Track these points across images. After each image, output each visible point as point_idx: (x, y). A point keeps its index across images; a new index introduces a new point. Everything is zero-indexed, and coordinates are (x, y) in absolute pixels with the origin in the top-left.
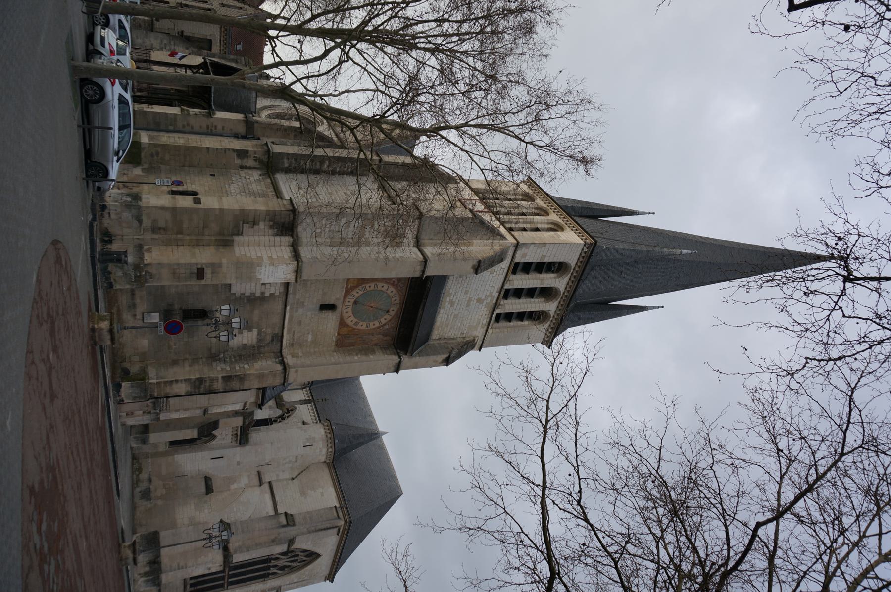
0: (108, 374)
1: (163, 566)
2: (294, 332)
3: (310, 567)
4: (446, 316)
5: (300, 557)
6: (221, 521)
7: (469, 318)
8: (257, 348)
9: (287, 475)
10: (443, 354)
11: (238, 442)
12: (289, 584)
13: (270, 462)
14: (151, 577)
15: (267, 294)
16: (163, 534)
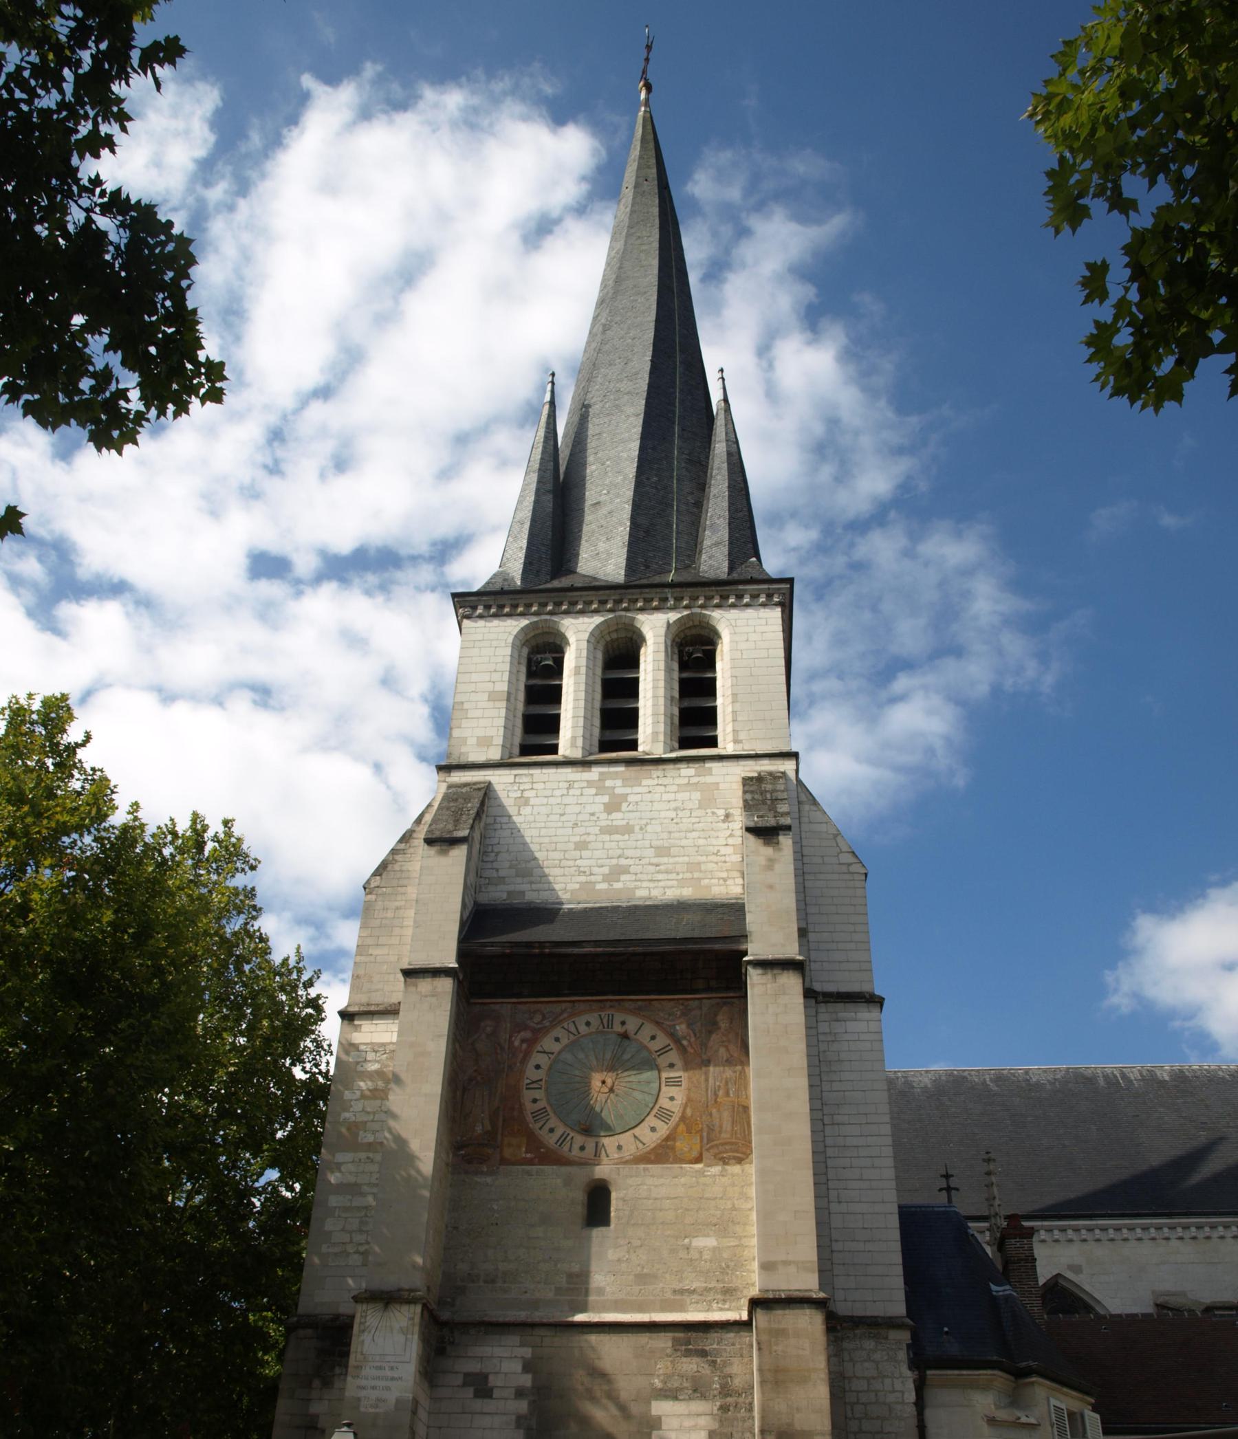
2: (682, 1292)
4: (660, 877)
7: (673, 814)
8: (729, 1399)
15: (527, 1380)
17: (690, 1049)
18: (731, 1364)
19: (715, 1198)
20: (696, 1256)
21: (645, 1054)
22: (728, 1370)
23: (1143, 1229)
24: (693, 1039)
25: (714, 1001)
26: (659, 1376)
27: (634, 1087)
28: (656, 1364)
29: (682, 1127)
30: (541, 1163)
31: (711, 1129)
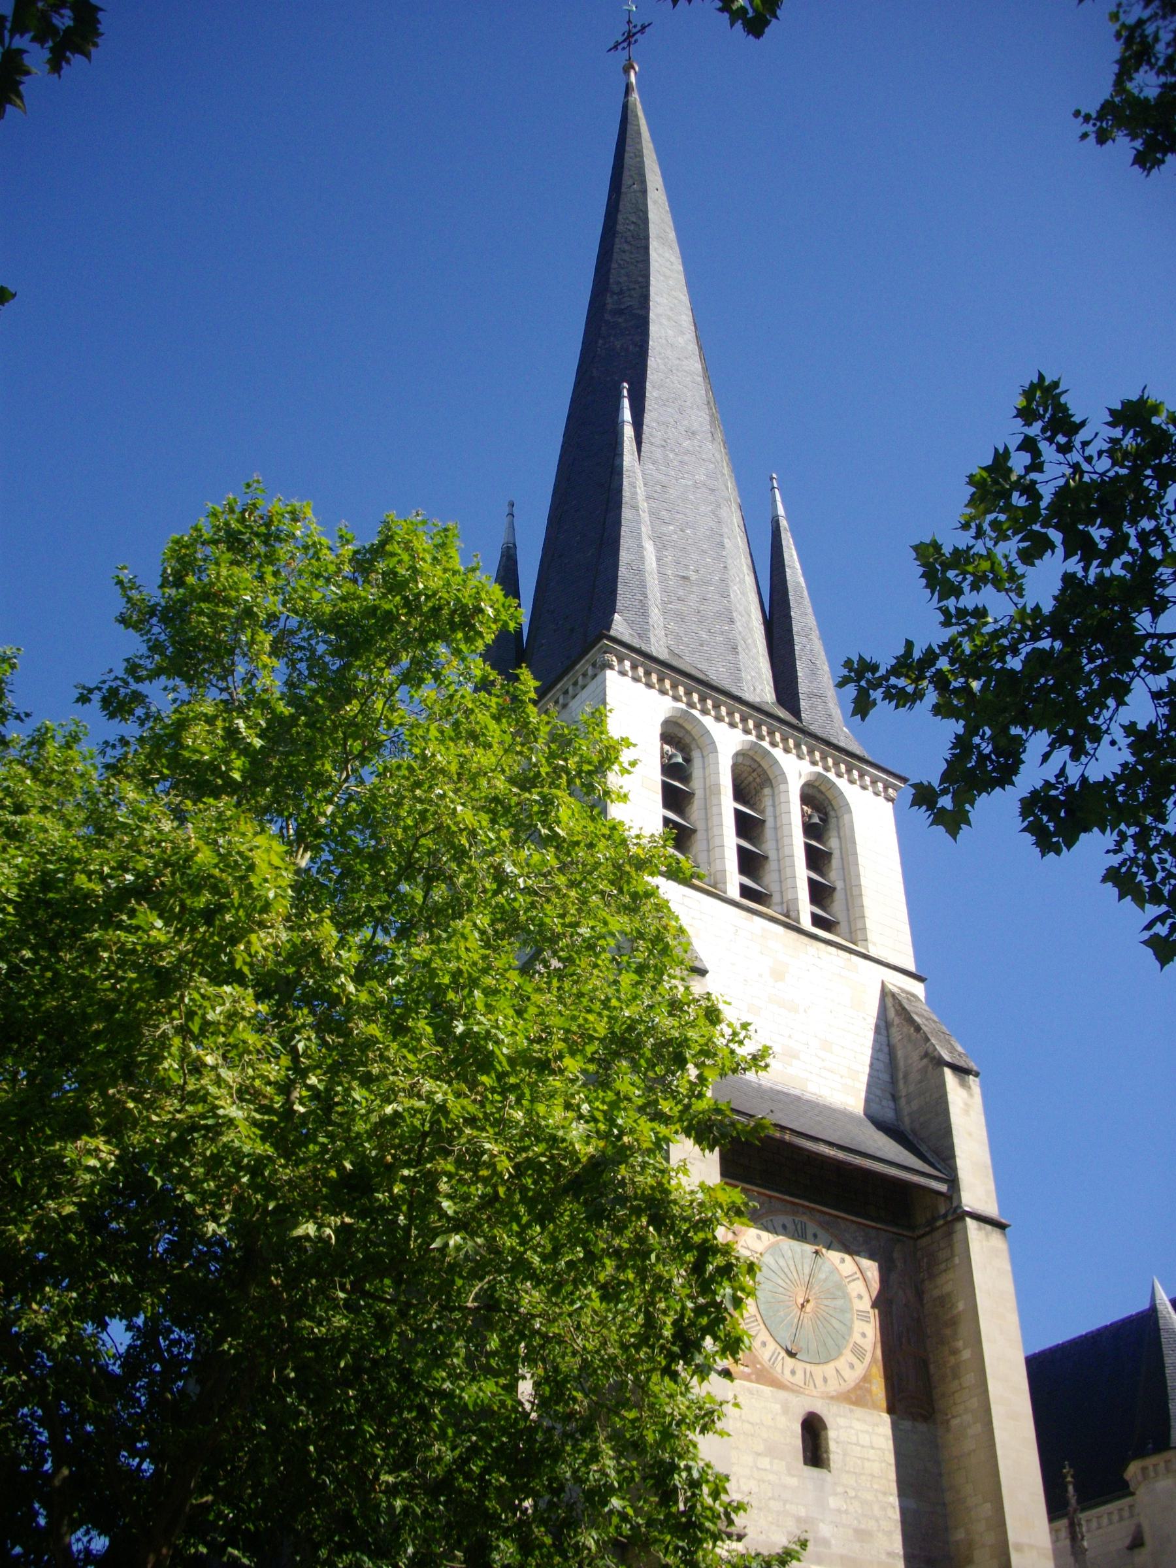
10: (942, 1085)
30: (758, 1381)
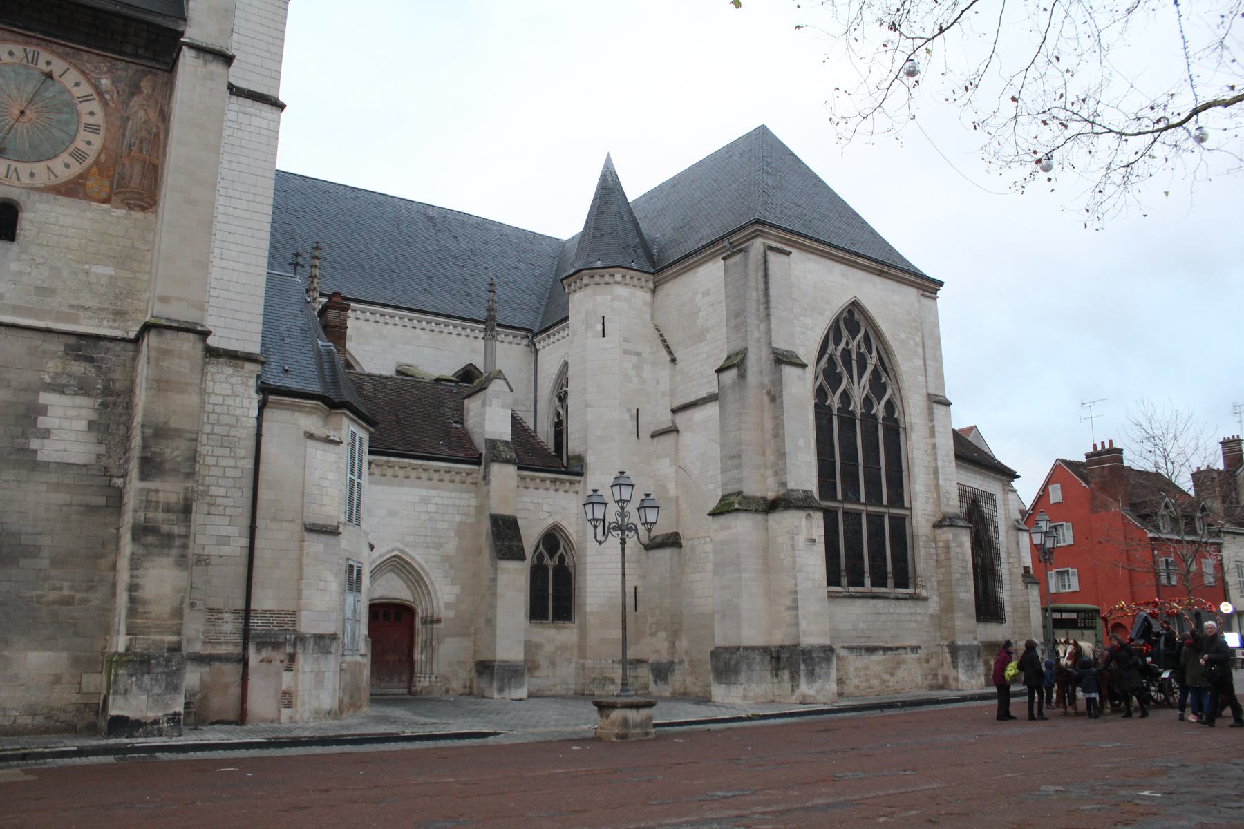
0: (72, 744)
1: (787, 642)
2: (77, 307)
3: (884, 327)
5: (853, 346)
6: (713, 514)
8: (109, 399)
9: (665, 372)
11: (578, 478)
12: (926, 376)
13: (629, 410)
14: (802, 667)
16: (720, 641)
17: (111, 104)
18: (114, 371)
19: (117, 236)
20: (94, 280)
21: (66, 97)
22: (111, 376)
23: (400, 318)
24: (115, 96)
25: (141, 68)
26: (48, 373)
27: (53, 124)
28: (47, 363)
29: (95, 169)
31: (122, 177)
